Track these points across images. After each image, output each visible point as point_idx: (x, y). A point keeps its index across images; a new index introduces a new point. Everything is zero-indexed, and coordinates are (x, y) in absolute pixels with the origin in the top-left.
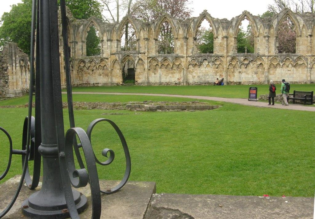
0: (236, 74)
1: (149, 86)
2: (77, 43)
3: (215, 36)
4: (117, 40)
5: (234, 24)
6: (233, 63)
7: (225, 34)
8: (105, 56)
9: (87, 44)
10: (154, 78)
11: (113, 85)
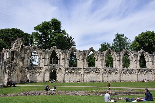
3: (96, 59)
4: (48, 58)
10: (67, 79)
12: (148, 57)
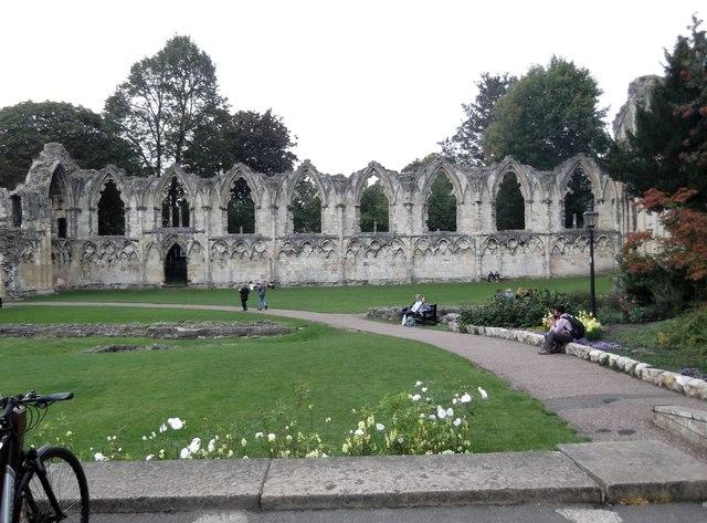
0: (360, 266)
1: (211, 291)
2: (80, 211)
3: (323, 204)
4: (155, 209)
5: (354, 183)
6: (355, 249)
7: (339, 201)
8: (132, 235)
9: (99, 213)
11: (147, 287)
12: (530, 184)
